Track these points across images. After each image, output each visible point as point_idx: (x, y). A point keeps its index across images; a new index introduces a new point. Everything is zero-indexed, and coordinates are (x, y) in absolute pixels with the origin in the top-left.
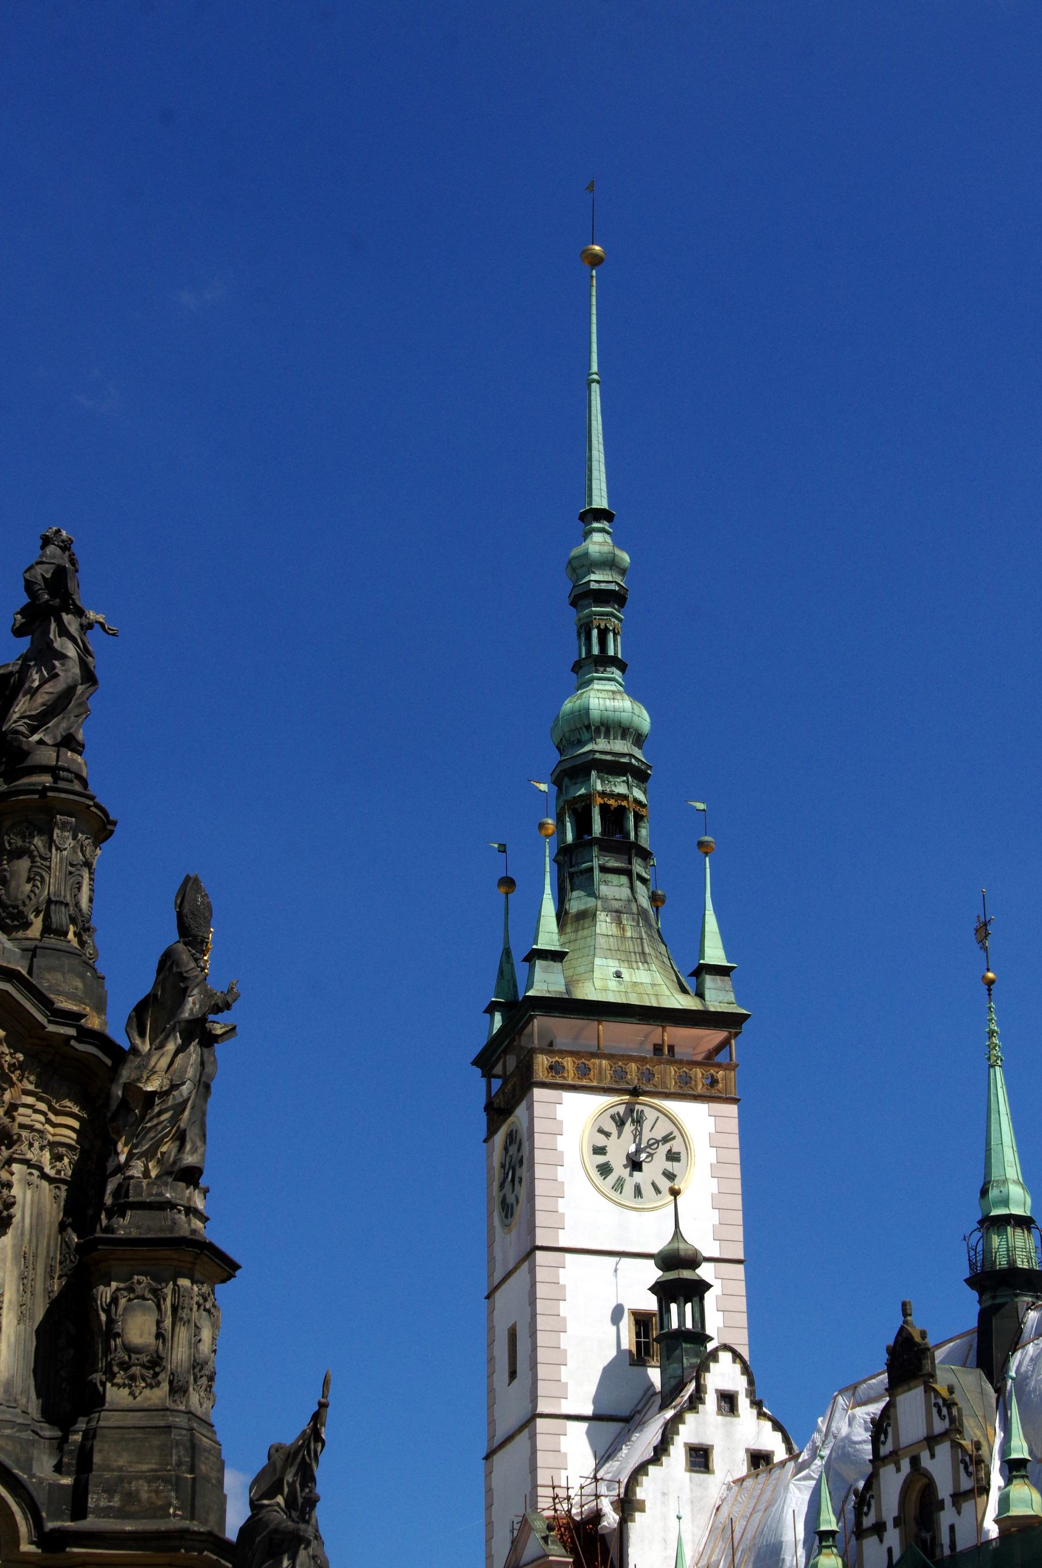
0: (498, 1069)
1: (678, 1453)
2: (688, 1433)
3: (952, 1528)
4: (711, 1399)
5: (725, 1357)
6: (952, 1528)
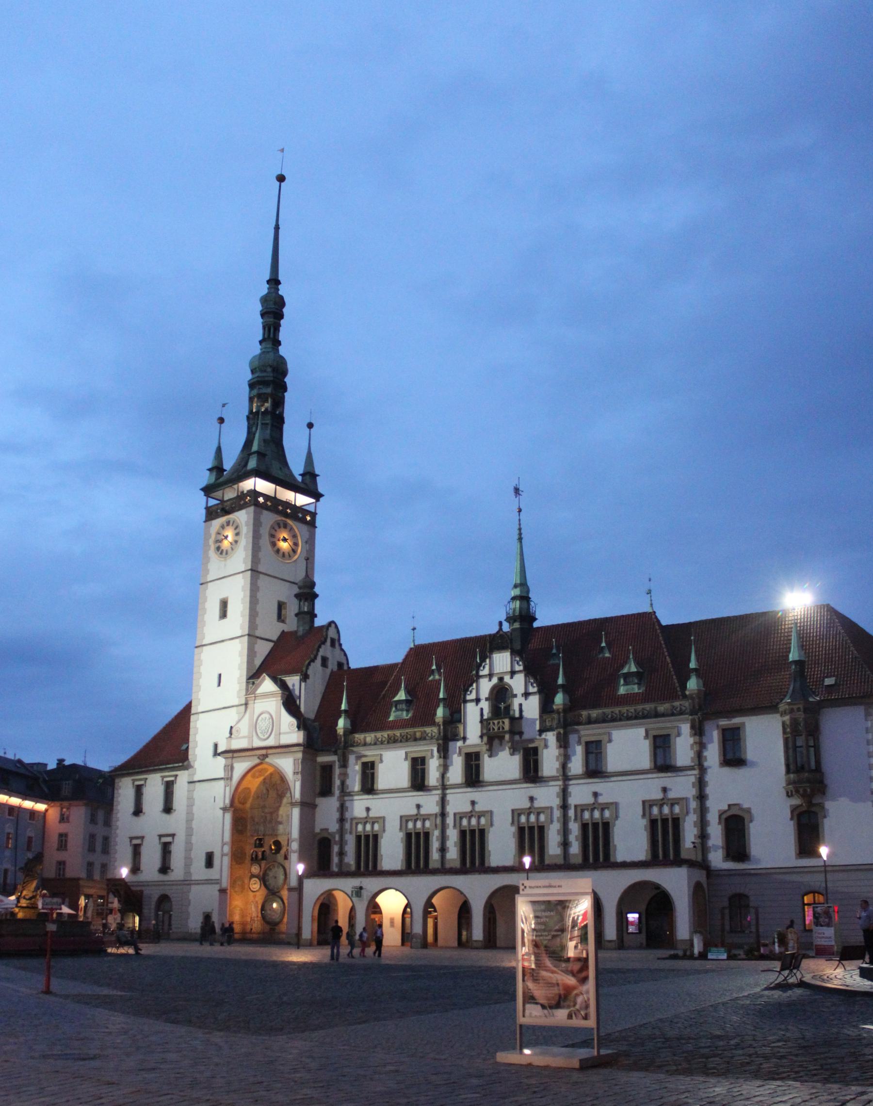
0: (218, 494)
1: (319, 661)
2: (321, 653)
3: (521, 705)
4: (329, 641)
5: (333, 625)
6: (521, 705)
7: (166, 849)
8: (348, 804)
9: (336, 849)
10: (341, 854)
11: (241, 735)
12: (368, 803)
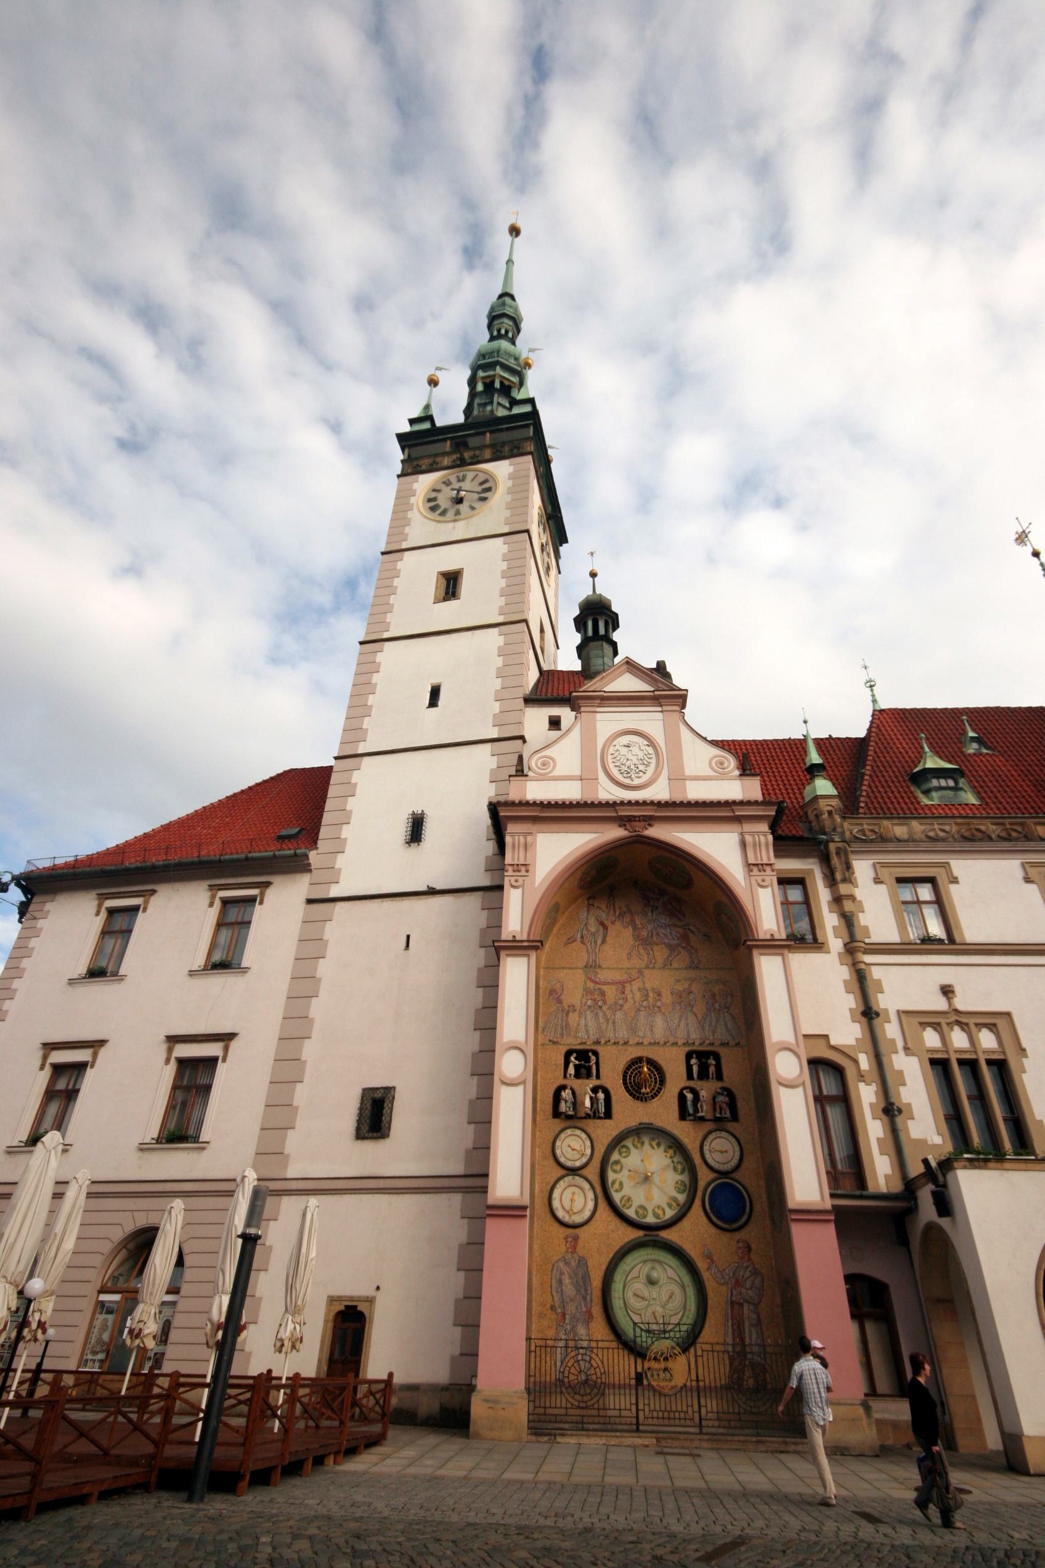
7: (193, 1079)
8: (876, 973)
9: (866, 1095)
10: (890, 1111)
11: (555, 773)
12: (946, 976)
